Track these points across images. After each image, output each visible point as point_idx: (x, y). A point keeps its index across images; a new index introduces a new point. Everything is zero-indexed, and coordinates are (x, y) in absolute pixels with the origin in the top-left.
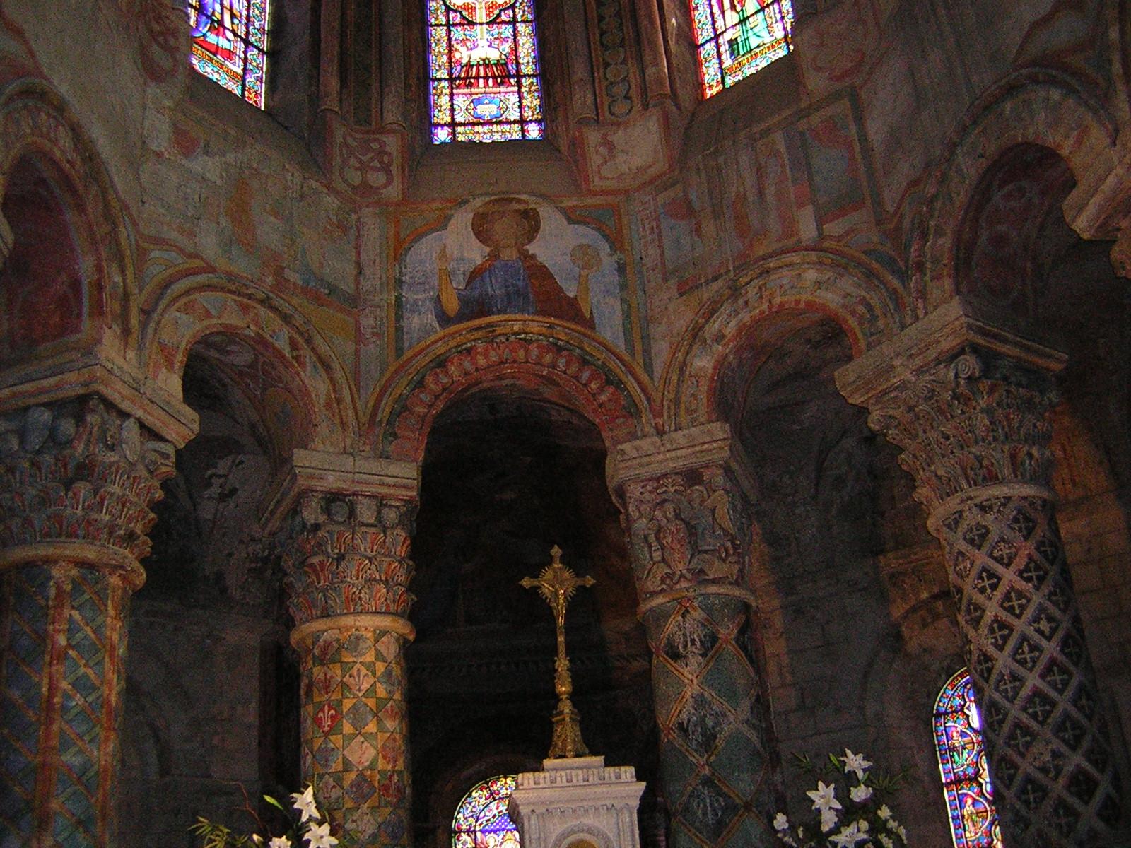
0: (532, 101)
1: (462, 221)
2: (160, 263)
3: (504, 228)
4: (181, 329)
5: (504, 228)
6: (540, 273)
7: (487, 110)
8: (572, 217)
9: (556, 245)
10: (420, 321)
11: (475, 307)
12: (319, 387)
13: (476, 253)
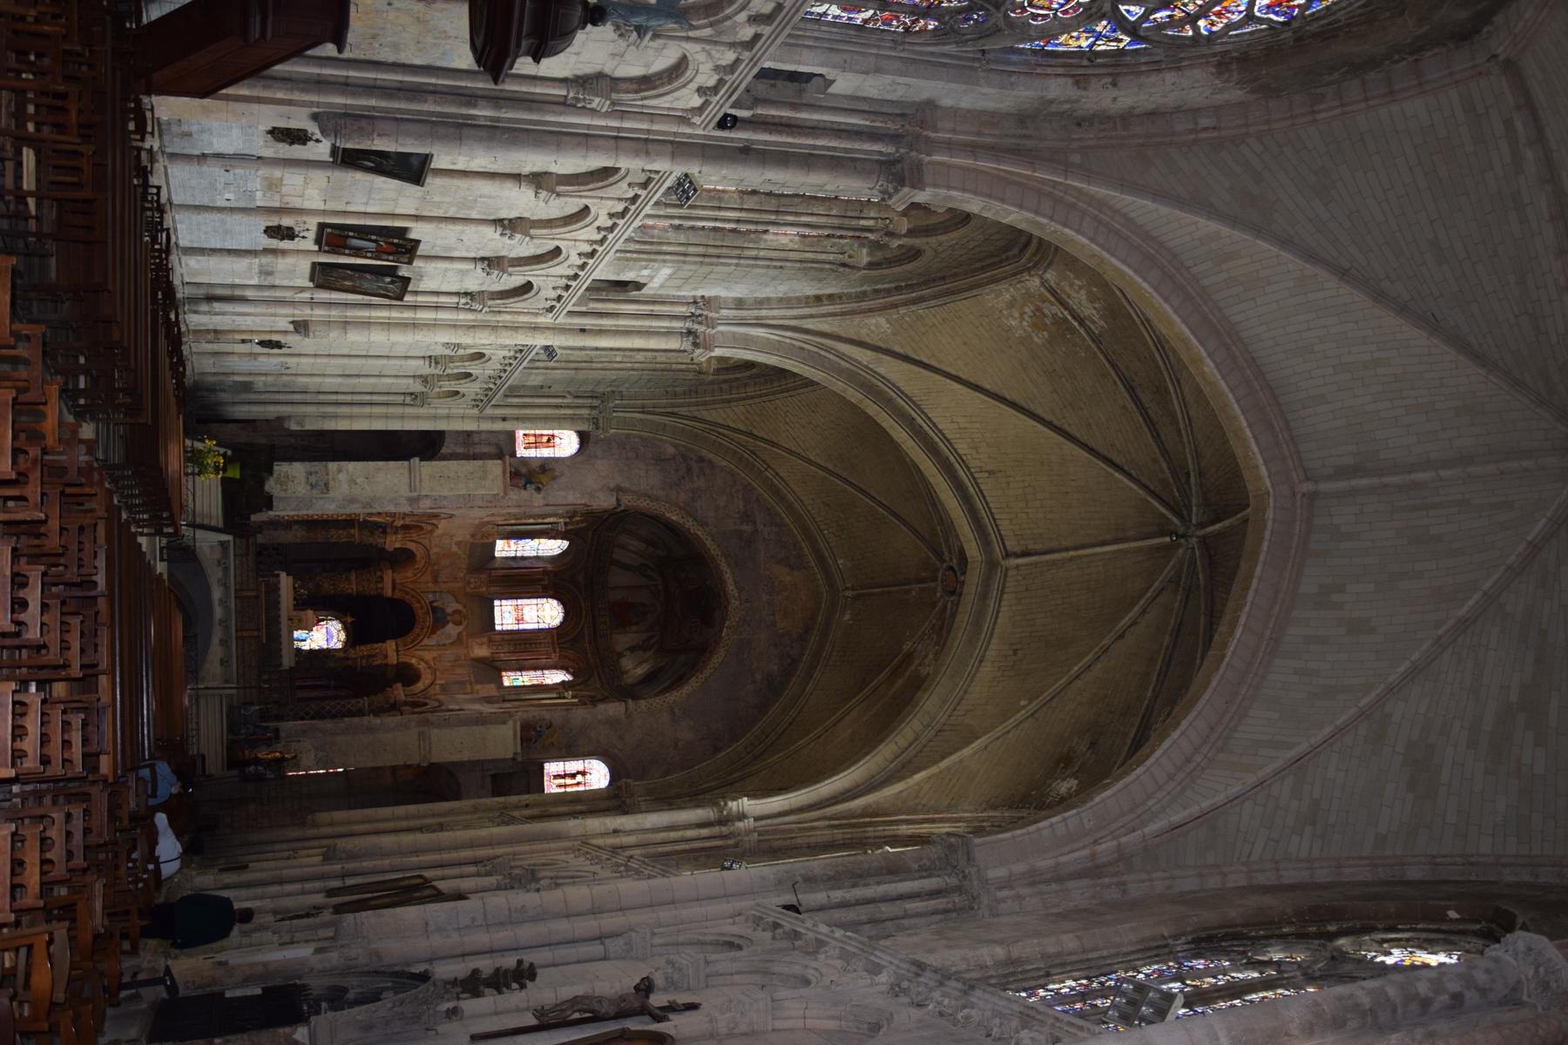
0: (509, 628)
1: (459, 607)
2: (426, 542)
3: (457, 617)
4: (412, 546)
5: (457, 617)
6: (444, 626)
7: (506, 615)
8: (459, 634)
9: (452, 630)
10: (431, 596)
11: (435, 610)
12: (409, 574)
13: (449, 610)
